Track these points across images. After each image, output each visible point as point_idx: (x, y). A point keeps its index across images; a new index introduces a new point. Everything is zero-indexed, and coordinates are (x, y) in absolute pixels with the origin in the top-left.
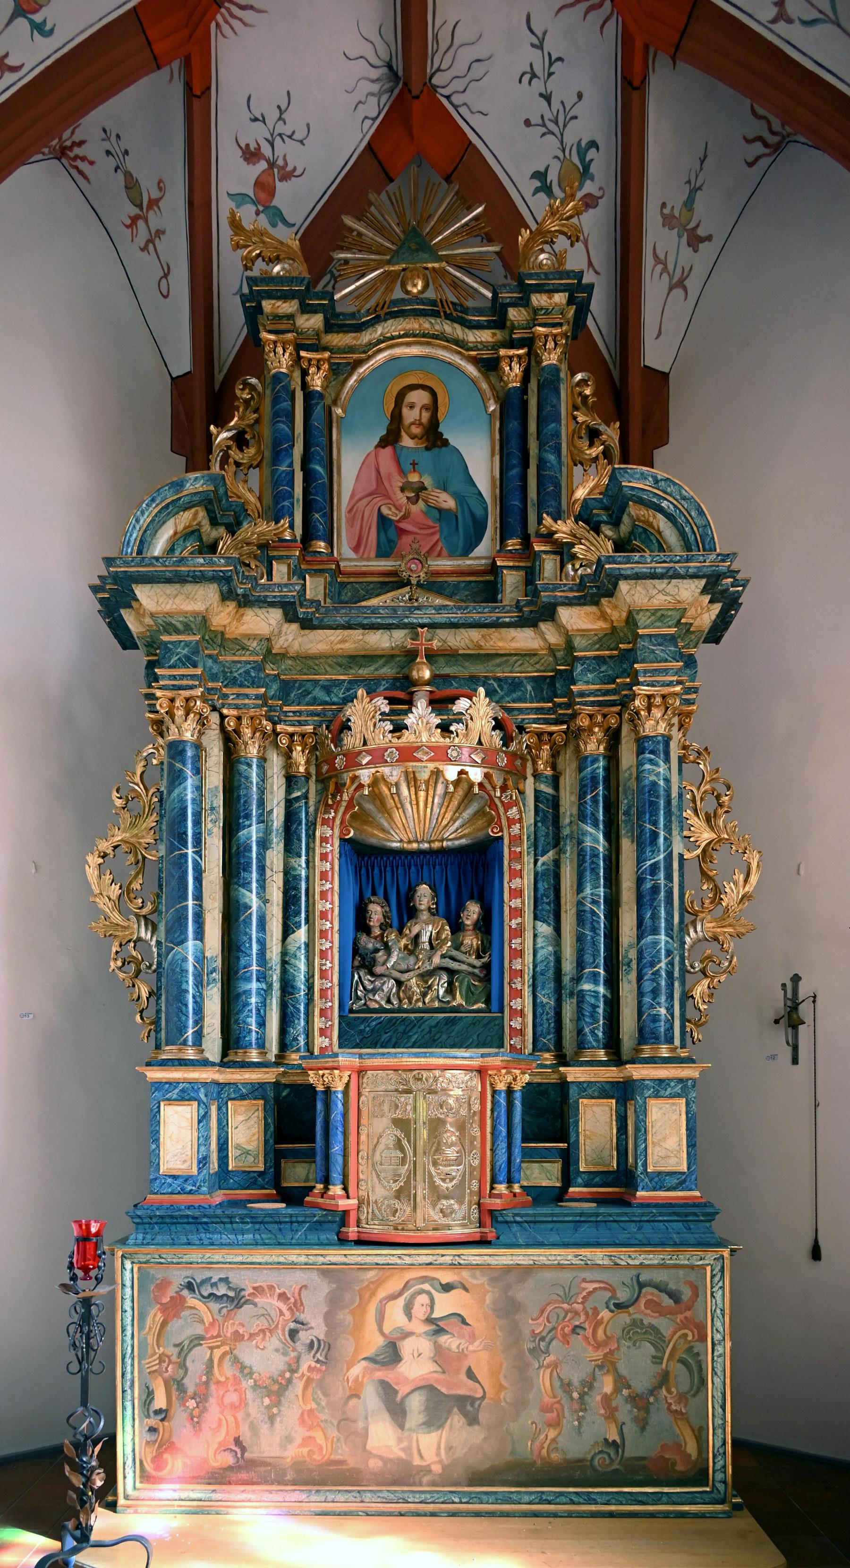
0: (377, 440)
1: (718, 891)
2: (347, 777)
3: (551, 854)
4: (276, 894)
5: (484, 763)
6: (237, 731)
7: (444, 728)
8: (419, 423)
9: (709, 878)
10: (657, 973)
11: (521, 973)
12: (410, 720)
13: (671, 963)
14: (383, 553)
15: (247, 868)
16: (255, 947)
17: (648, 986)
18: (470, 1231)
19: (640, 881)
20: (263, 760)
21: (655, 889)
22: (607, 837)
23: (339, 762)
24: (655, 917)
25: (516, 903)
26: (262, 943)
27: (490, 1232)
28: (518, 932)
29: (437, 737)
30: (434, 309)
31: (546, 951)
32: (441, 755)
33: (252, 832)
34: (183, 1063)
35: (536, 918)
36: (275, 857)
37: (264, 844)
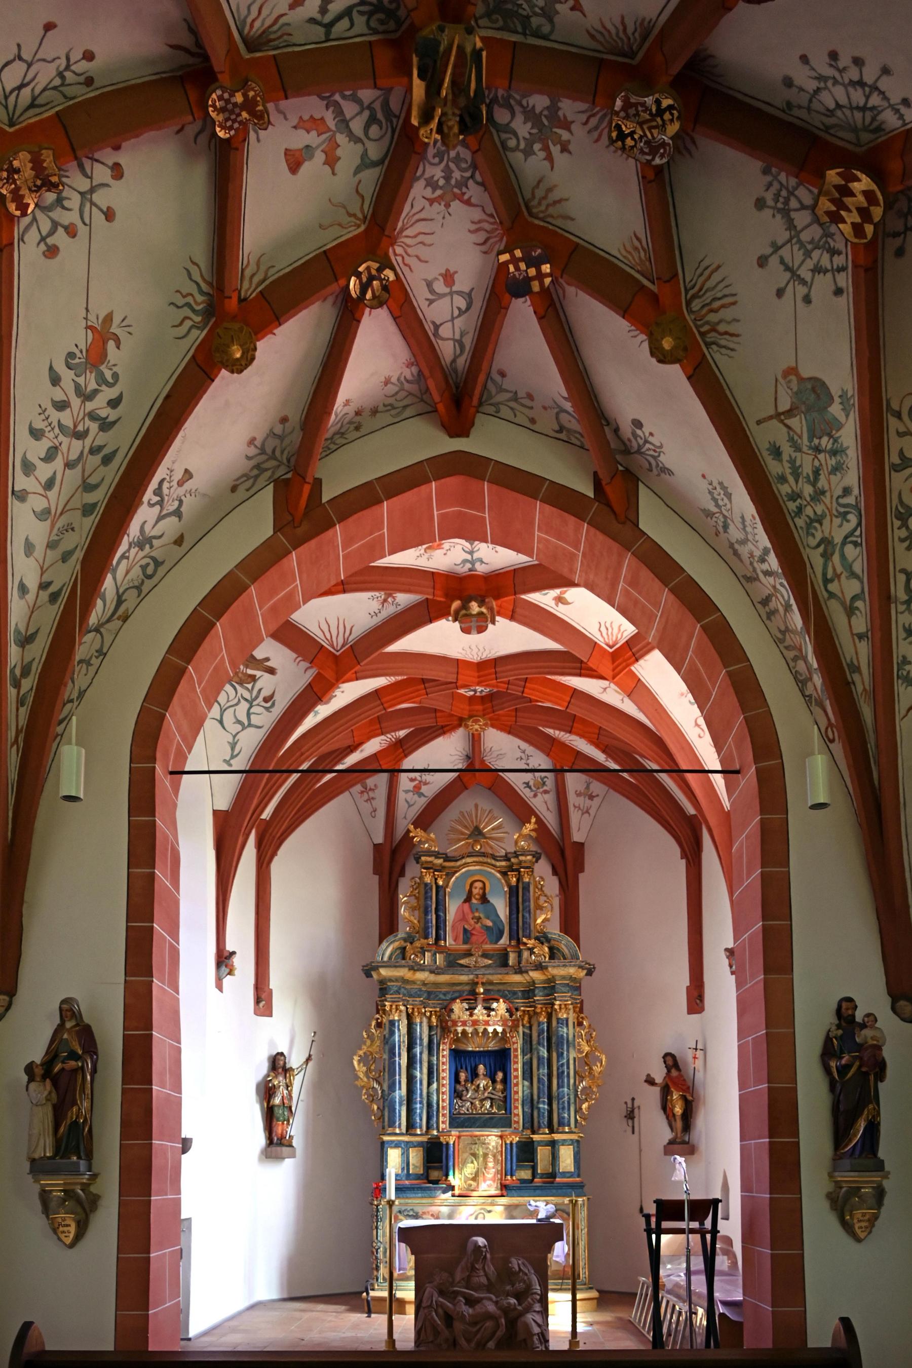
0: (462, 900)
1: (591, 1069)
2: (452, 1029)
3: (528, 1056)
4: (425, 1070)
5: (502, 1025)
6: (412, 1013)
7: (489, 1016)
8: (478, 894)
9: (588, 1065)
10: (564, 1102)
11: (518, 1100)
12: (476, 1011)
13: (569, 1098)
14: (465, 942)
15: (416, 1063)
16: (419, 1092)
17: (561, 1106)
18: (498, 1192)
19: (558, 1069)
20: (421, 1023)
21: (563, 1072)
22: (548, 1051)
23: (450, 1023)
24: (563, 1082)
25: (515, 1074)
26: (421, 1090)
27: (505, 1192)
28: (517, 1085)
29: (486, 1018)
30: (484, 855)
31: (527, 1092)
32: (487, 1023)
33: (418, 1050)
34: (396, 1134)
35: (524, 1079)
36: (425, 1057)
37: (421, 1053)
